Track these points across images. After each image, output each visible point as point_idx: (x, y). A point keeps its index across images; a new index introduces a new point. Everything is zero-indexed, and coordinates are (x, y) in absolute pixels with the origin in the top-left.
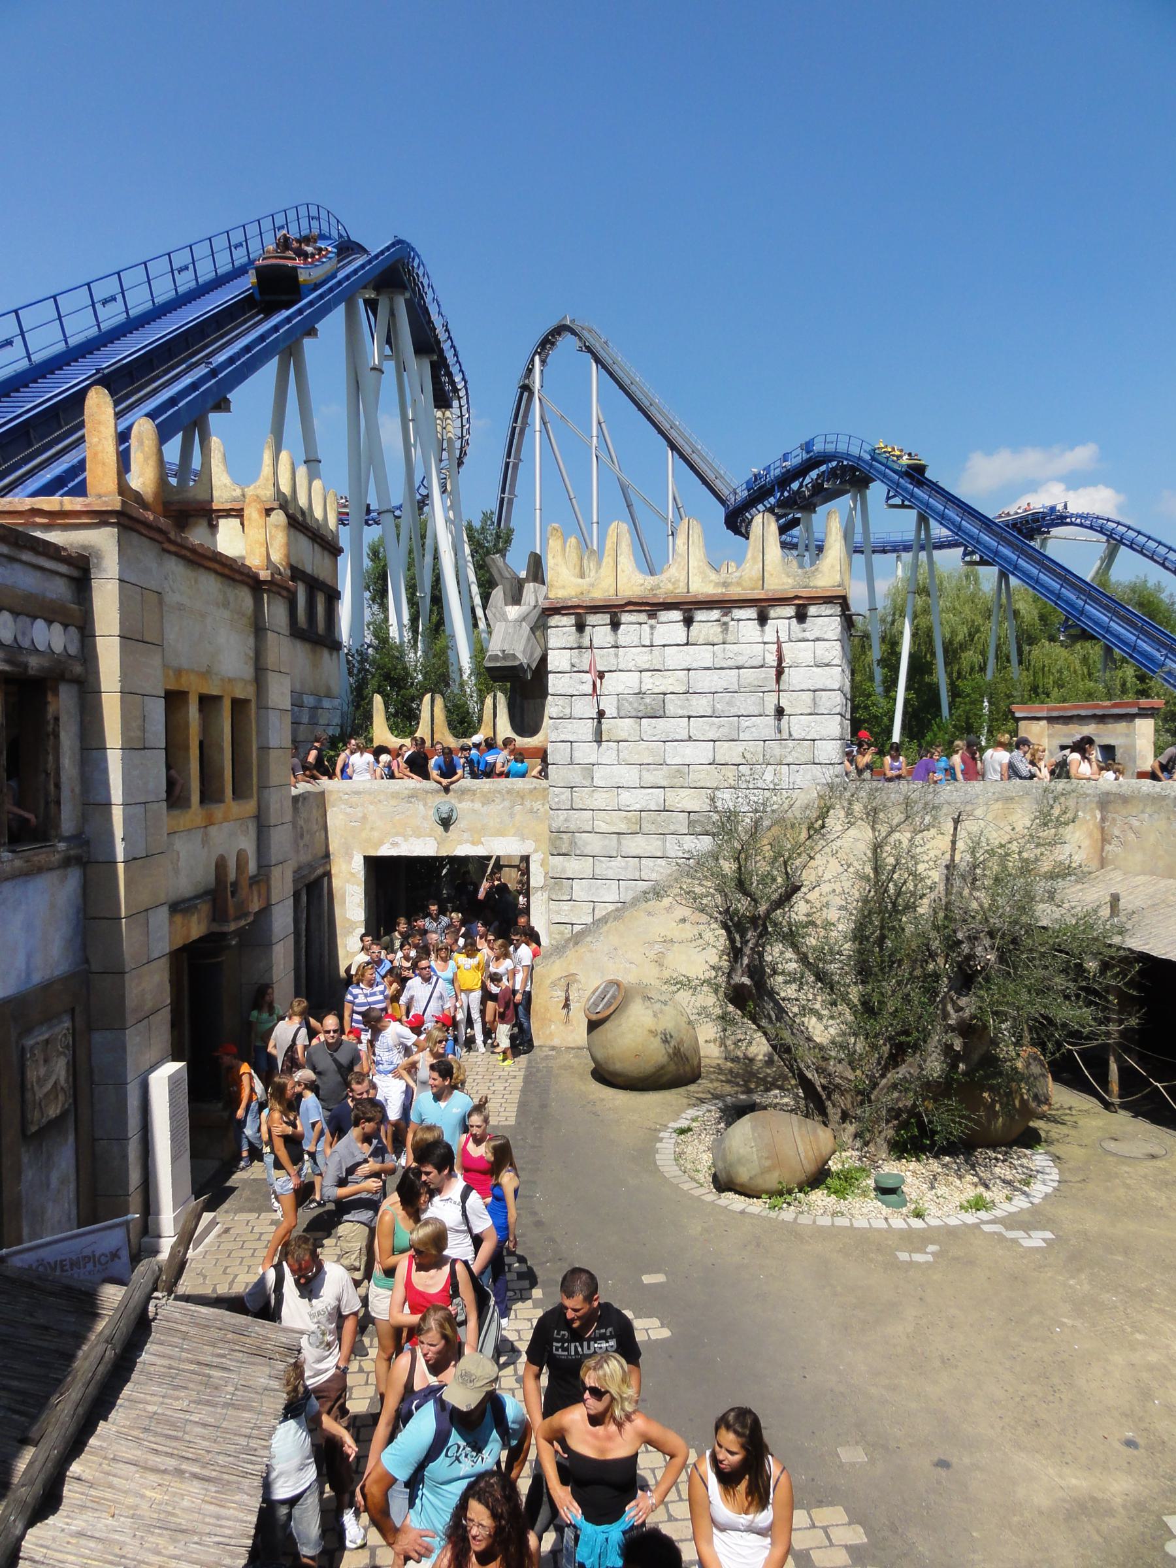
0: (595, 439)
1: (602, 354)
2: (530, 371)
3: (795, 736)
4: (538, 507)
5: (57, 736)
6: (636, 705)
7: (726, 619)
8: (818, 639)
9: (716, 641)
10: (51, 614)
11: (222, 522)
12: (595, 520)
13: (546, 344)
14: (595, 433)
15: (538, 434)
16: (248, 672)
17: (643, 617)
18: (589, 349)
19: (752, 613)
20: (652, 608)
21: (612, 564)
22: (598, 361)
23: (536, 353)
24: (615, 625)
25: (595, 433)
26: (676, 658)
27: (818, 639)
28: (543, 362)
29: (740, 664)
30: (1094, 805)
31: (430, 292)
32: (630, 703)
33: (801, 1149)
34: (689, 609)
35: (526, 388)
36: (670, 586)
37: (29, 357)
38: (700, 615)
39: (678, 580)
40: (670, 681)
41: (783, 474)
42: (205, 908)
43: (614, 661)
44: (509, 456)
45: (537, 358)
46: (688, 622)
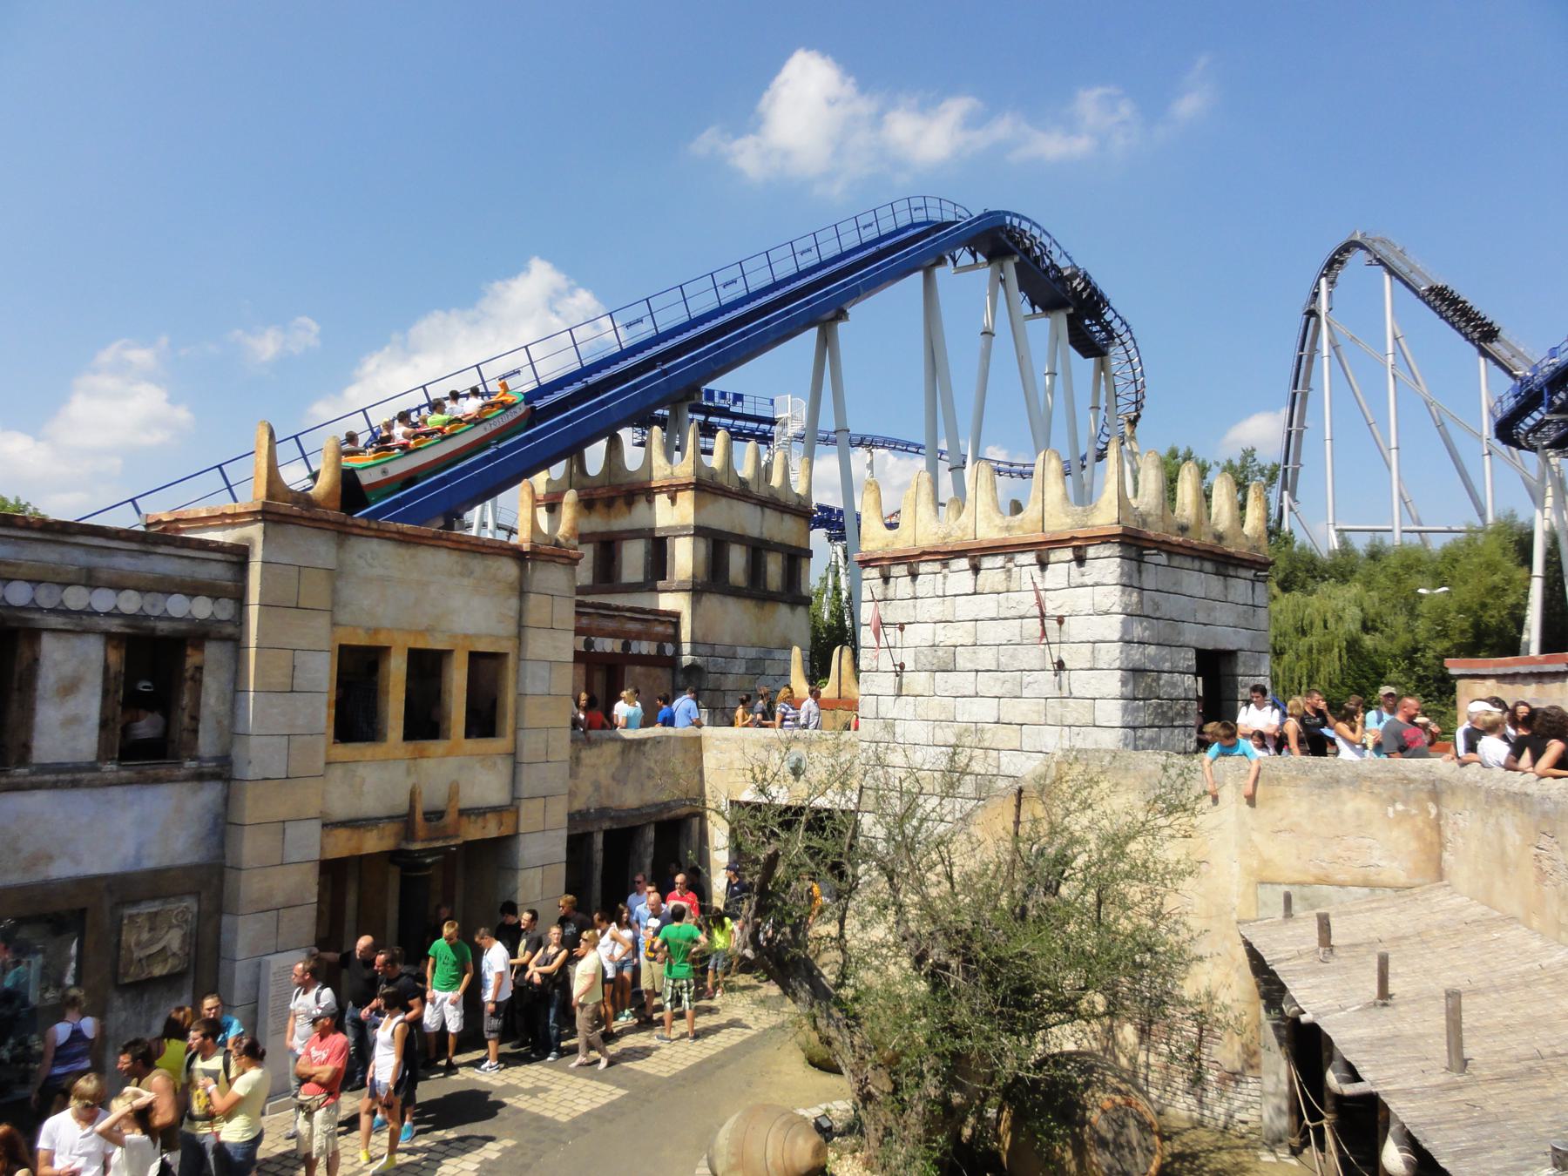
0: (1390, 358)
1: (1396, 263)
2: (1316, 295)
3: (1075, 694)
4: (1328, 436)
5: (197, 682)
6: (930, 658)
7: (1010, 565)
8: (1096, 585)
9: (1001, 589)
10: (212, 591)
11: (657, 497)
12: (1393, 444)
13: (1334, 264)
14: (1390, 350)
15: (1326, 360)
16: (511, 628)
17: (937, 567)
18: (1380, 262)
19: (1030, 558)
20: (945, 556)
21: (912, 514)
22: (1392, 272)
23: (1322, 275)
24: (914, 575)
25: (1390, 350)
26: (967, 608)
27: (1096, 585)
28: (1332, 283)
29: (1022, 613)
30: (1423, 796)
31: (1054, 248)
32: (926, 656)
33: (770, 1154)
34: (976, 555)
35: (1312, 313)
36: (960, 534)
37: (537, 379)
38: (987, 563)
39: (966, 527)
40: (960, 632)
41: (1553, 373)
42: (391, 828)
43: (912, 613)
44: (1296, 387)
45: (1323, 281)
46: (976, 569)
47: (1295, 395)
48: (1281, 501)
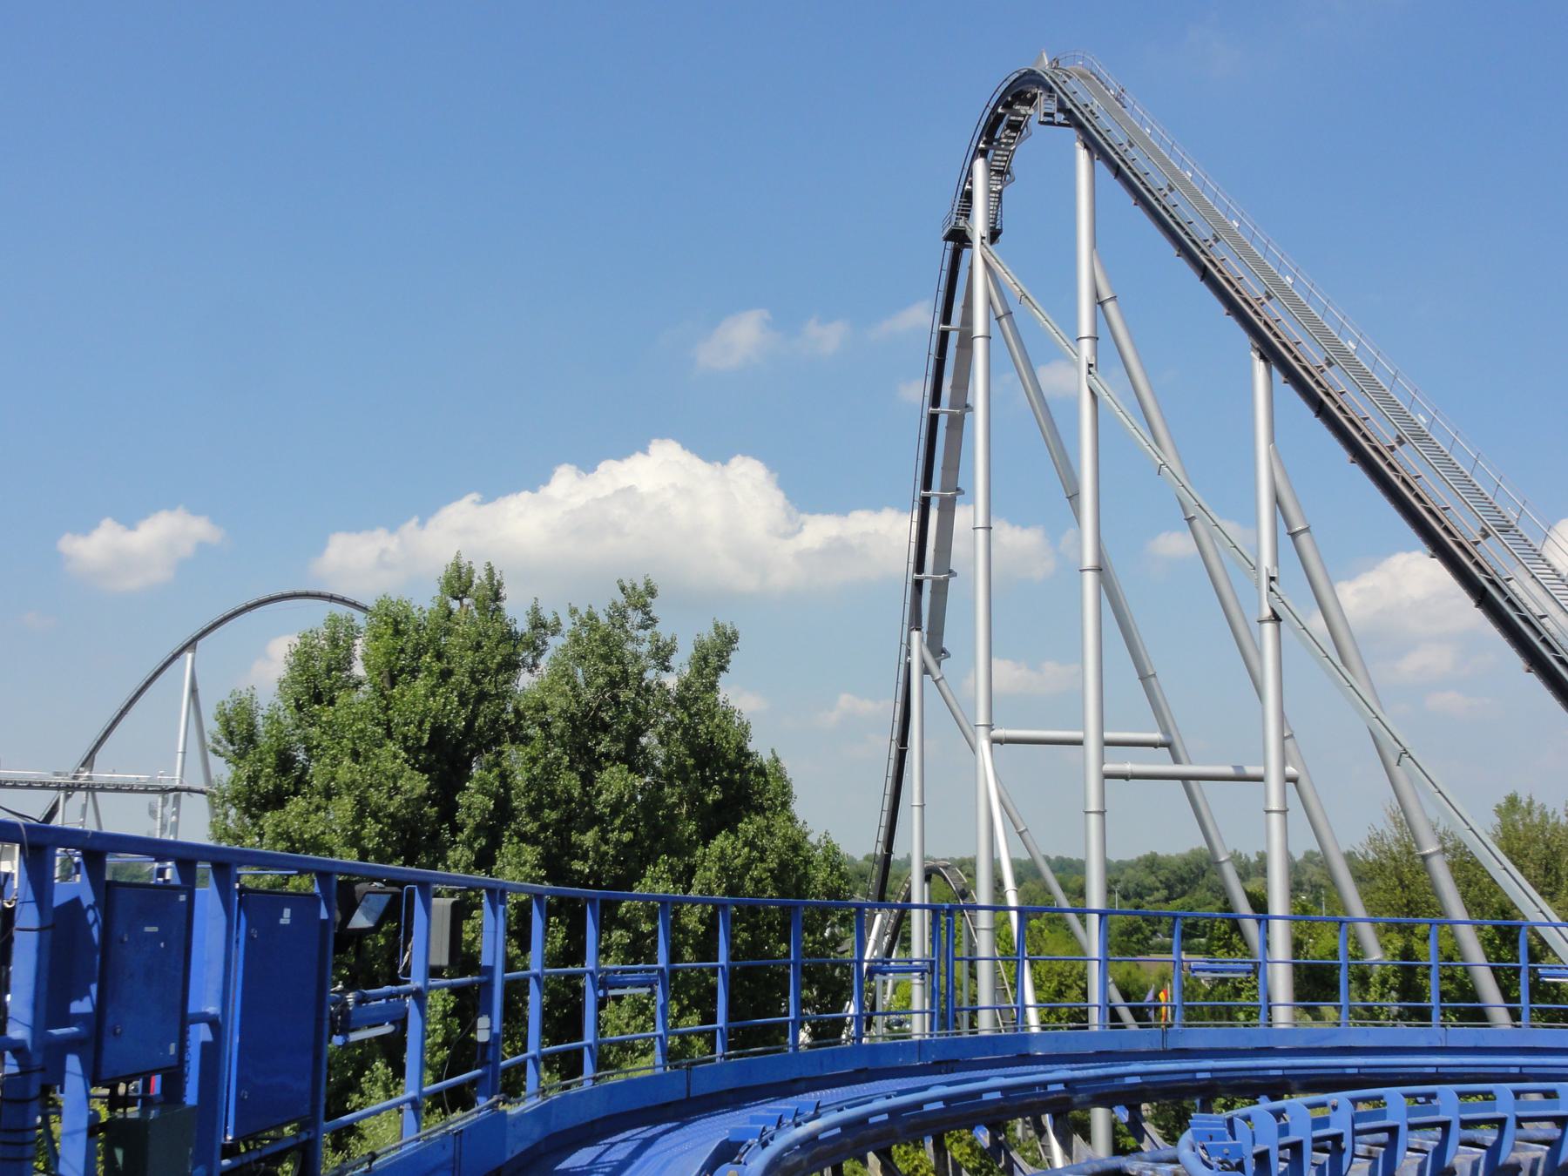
0: (1086, 346)
18: (1072, 120)
25: (1085, 329)
28: (1000, 173)
45: (979, 164)
47: (934, 419)
48: (909, 653)
